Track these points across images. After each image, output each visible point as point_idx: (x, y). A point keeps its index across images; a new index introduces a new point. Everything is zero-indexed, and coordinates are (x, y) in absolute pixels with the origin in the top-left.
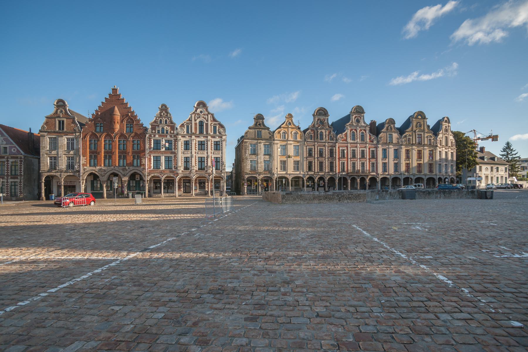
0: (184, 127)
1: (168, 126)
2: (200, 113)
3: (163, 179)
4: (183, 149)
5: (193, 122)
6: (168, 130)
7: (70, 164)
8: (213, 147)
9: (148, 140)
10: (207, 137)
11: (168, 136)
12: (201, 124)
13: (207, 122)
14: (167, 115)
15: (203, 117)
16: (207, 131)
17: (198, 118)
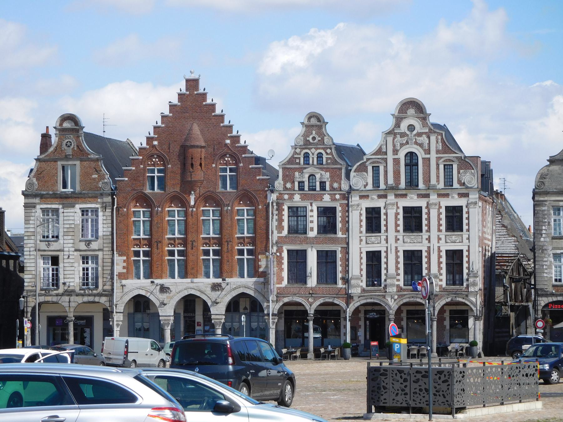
0: (367, 172)
1: (327, 170)
2: (408, 133)
3: (311, 311)
4: (364, 229)
5: (390, 157)
6: (323, 180)
7: (87, 274)
8: (443, 222)
9: (275, 207)
10: (427, 196)
11: (327, 198)
12: (411, 160)
13: (428, 156)
14: (322, 141)
15: (416, 143)
16: (427, 180)
17: (402, 145)
